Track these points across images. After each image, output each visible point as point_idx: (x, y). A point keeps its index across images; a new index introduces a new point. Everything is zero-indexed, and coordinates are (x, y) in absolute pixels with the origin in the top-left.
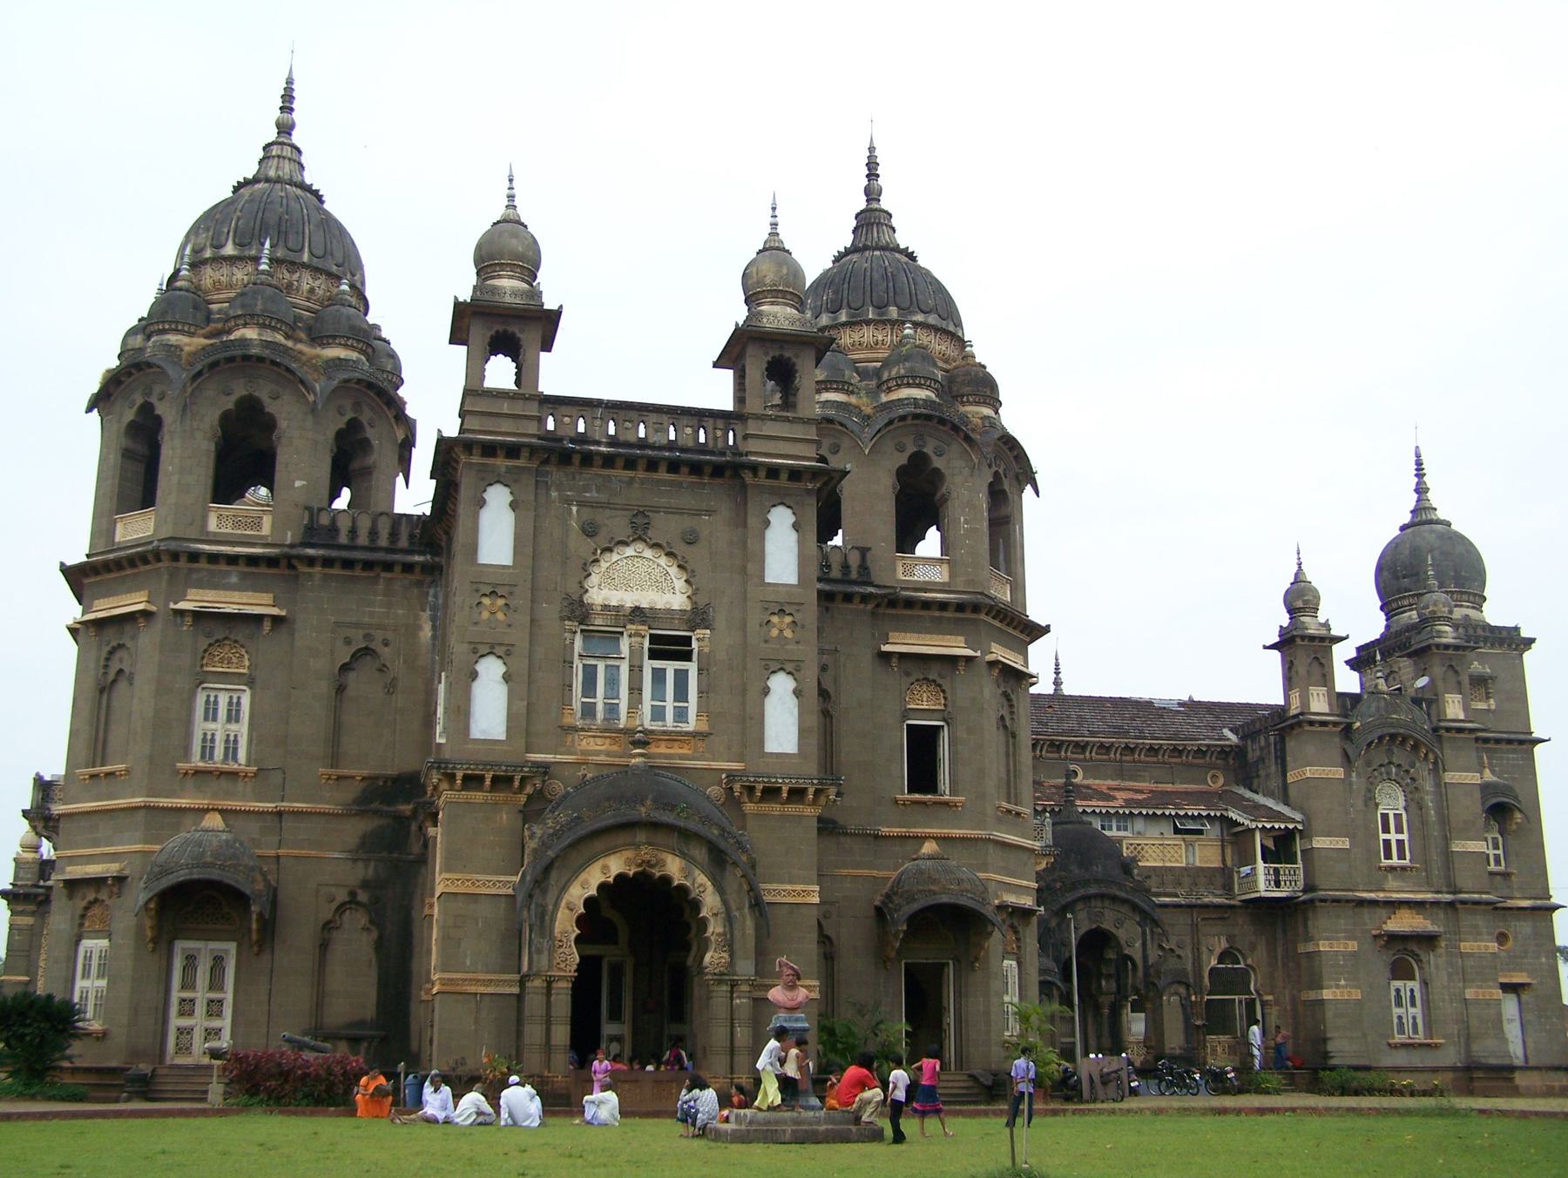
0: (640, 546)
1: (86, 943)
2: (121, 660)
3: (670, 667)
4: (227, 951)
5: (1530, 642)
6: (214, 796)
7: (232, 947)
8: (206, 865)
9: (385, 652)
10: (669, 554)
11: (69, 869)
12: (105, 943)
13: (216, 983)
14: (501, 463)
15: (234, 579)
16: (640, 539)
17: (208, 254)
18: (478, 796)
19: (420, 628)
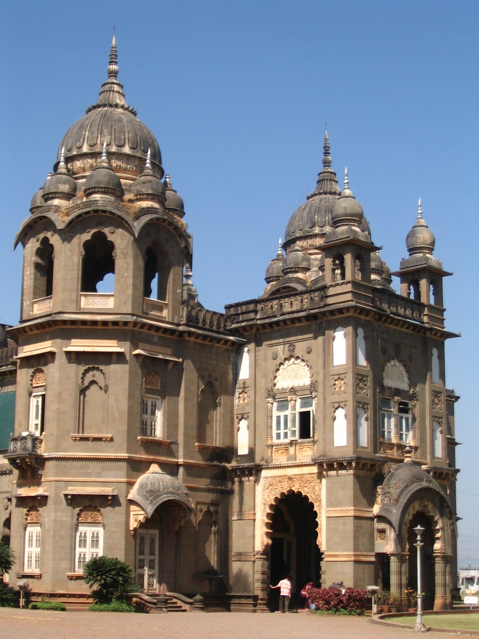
0: (396, 361)
1: (81, 529)
2: (94, 376)
3: (405, 415)
4: (155, 535)
5: (457, 398)
6: (152, 454)
7: (156, 532)
8: (171, 493)
9: (216, 384)
10: (405, 366)
11: (70, 488)
12: (100, 530)
13: (152, 553)
14: (363, 317)
15: (156, 339)
16: (397, 358)
17: (114, 149)
18: (362, 473)
19: (228, 373)
